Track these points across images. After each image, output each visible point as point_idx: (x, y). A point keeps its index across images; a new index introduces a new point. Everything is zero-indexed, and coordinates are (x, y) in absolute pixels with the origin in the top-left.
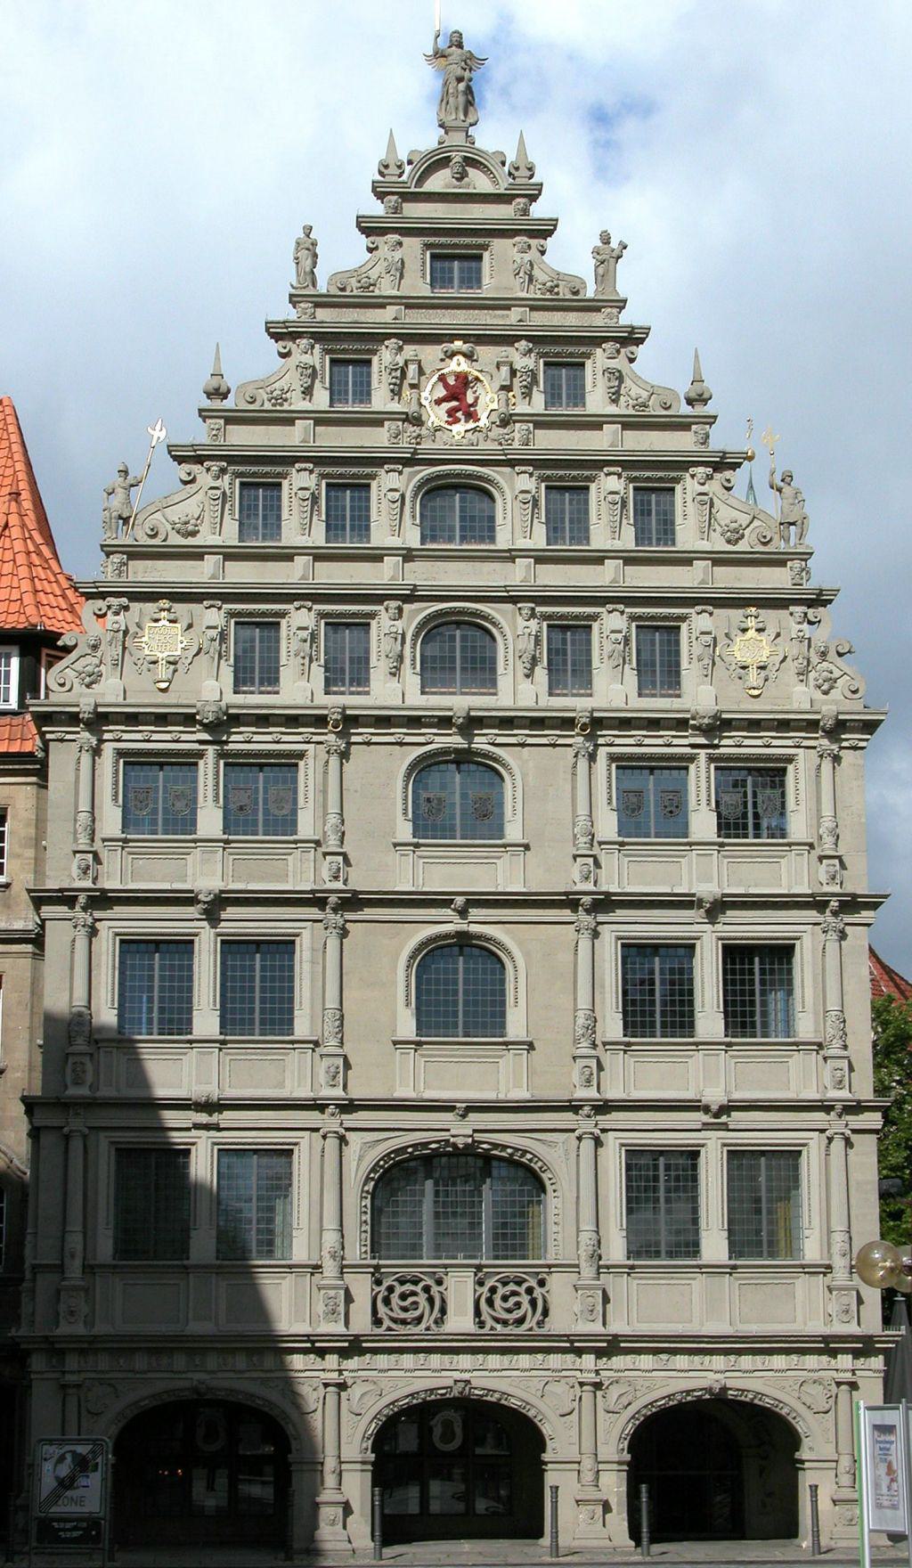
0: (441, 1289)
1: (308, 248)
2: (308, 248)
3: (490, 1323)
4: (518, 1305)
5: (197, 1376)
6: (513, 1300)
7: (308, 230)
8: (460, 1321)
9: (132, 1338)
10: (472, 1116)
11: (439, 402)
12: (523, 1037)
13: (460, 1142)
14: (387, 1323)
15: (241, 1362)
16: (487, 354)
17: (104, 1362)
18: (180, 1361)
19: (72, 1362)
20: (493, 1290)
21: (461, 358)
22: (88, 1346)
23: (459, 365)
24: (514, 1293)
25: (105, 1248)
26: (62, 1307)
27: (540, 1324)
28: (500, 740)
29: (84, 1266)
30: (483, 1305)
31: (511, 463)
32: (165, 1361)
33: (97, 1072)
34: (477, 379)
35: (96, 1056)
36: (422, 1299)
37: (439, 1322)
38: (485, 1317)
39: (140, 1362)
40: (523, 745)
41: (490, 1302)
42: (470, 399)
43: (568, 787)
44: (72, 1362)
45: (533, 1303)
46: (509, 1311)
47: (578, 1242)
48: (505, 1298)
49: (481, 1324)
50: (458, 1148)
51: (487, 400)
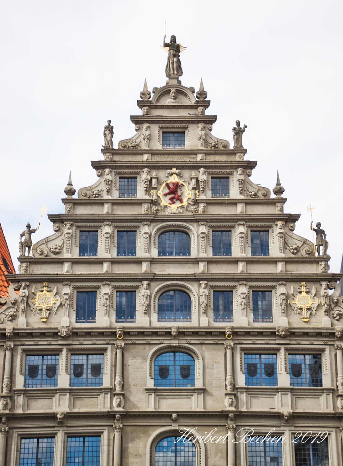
1: (109, 129)
2: (109, 129)
7: (110, 122)
11: (165, 195)
16: (186, 173)
23: (174, 179)
31: (197, 221)
42: (179, 193)
51: (188, 193)
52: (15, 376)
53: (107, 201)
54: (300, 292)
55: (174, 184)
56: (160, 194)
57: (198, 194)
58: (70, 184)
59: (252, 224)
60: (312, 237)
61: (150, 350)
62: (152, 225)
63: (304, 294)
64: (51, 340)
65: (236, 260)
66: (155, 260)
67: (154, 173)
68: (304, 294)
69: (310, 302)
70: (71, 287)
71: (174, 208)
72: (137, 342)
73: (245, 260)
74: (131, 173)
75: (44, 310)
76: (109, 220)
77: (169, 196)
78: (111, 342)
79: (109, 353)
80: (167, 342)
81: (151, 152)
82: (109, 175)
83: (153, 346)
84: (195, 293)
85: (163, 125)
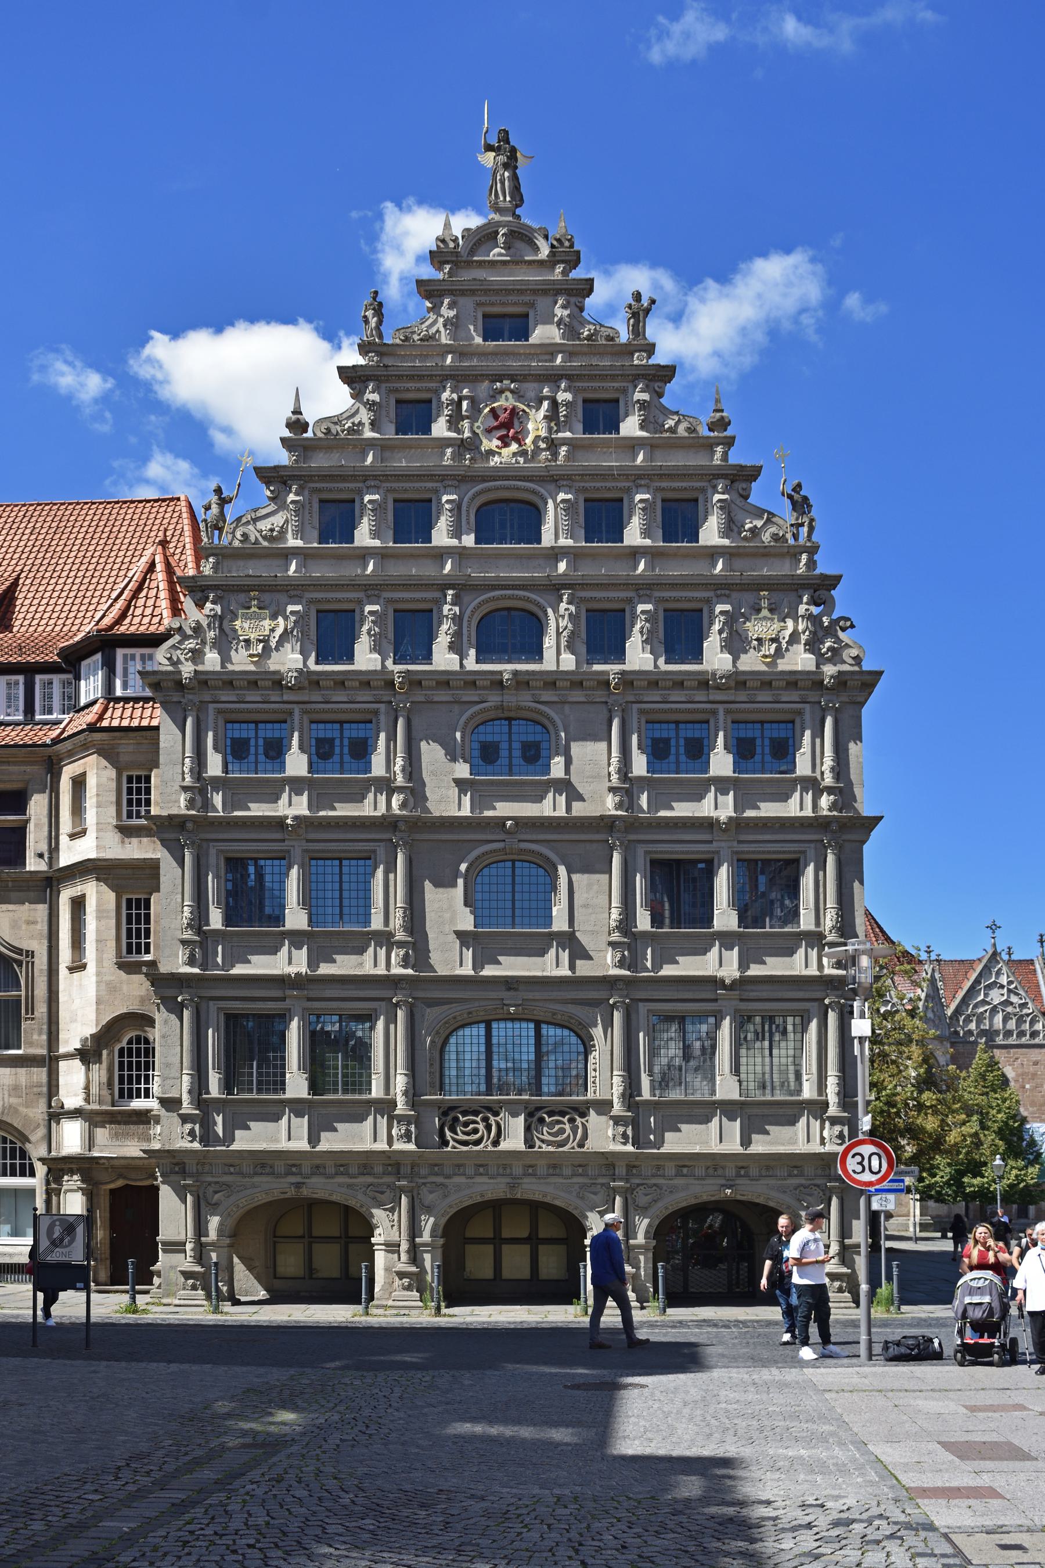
14: (451, 1143)
21: (508, 394)
36: (481, 1127)
54: (759, 611)
59: (664, 484)
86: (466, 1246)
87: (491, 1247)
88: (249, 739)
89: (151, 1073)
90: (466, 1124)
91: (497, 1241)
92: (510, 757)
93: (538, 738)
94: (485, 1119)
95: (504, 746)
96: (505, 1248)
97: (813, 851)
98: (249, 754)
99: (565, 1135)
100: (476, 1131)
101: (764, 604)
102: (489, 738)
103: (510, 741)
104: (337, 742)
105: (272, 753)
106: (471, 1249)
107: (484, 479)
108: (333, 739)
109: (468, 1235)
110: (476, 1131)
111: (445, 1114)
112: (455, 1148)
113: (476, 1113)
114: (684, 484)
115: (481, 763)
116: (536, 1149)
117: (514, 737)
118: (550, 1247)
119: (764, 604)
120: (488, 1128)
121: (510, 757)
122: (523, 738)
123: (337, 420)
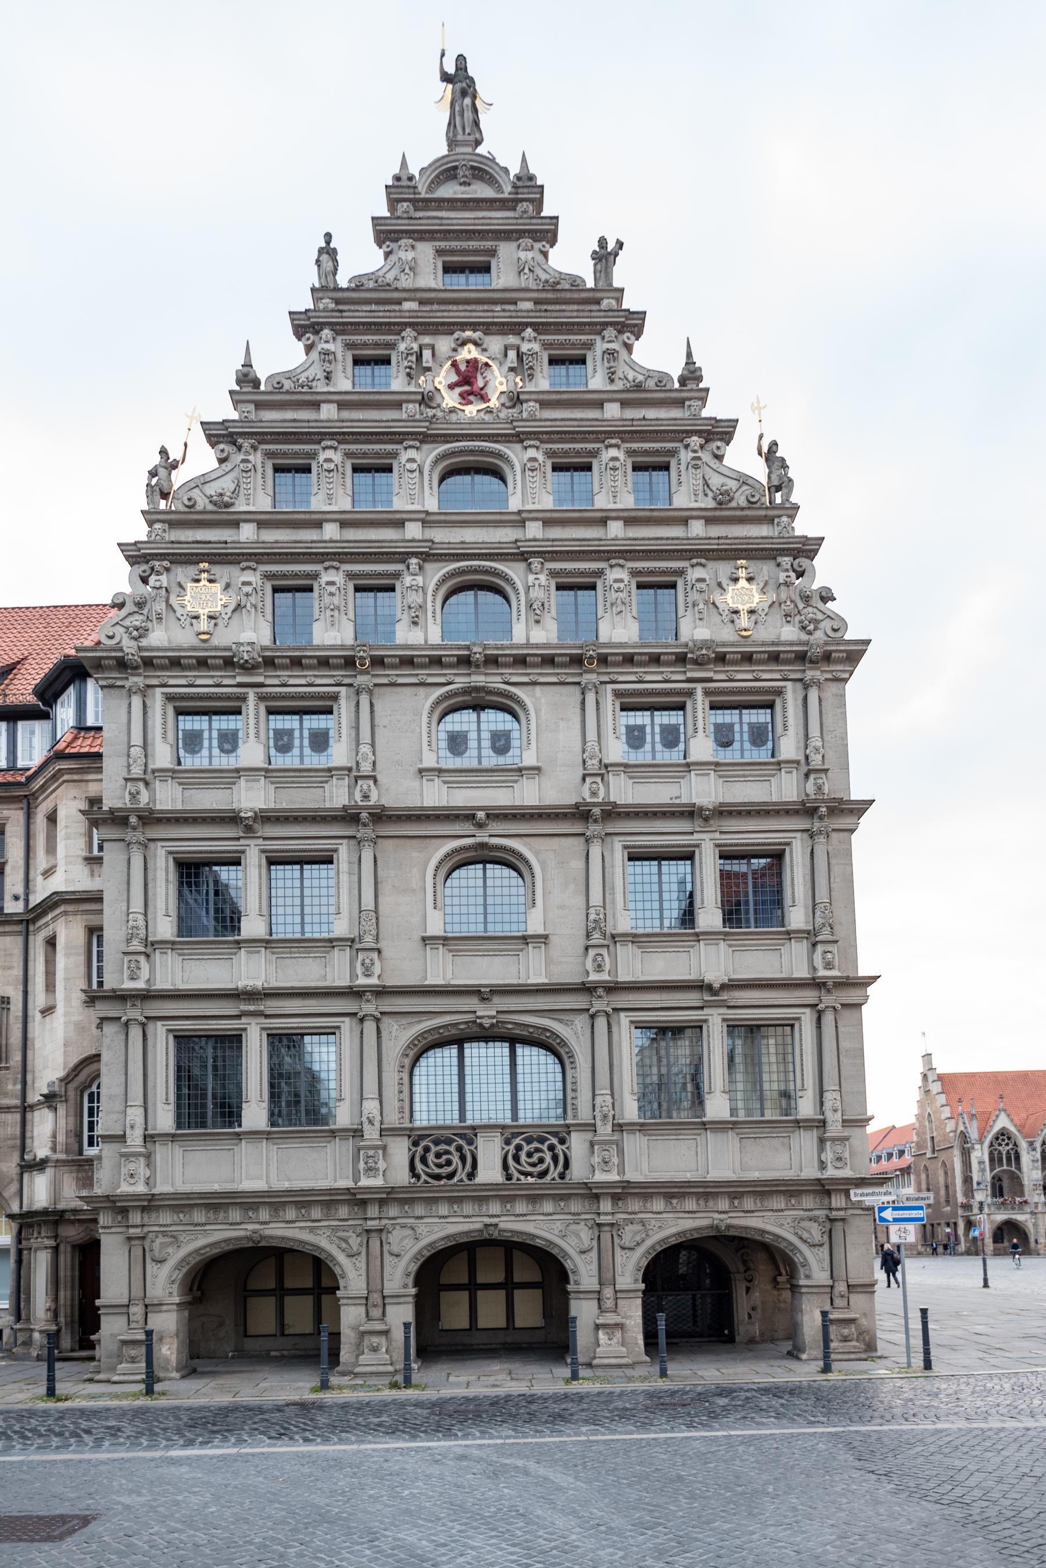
0: (472, 1148)
1: (328, 252)
2: (328, 252)
3: (516, 1175)
4: (541, 1161)
5: (250, 1227)
6: (536, 1156)
7: (328, 237)
8: (490, 1172)
9: (188, 1196)
10: (496, 999)
11: (451, 387)
12: (541, 931)
13: (487, 1022)
14: (424, 1177)
15: (291, 1214)
16: (495, 343)
17: (165, 1218)
18: (235, 1215)
19: (135, 1218)
20: (519, 1148)
21: (471, 346)
22: (150, 1204)
23: (469, 352)
24: (537, 1150)
25: (165, 1119)
26: (124, 1171)
27: (562, 1176)
28: (514, 679)
29: (145, 1137)
30: (511, 1161)
31: (518, 438)
32: (221, 1215)
33: (152, 970)
34: (487, 365)
35: (152, 956)
36: (456, 1159)
37: (471, 1175)
38: (512, 1170)
39: (199, 1216)
40: (534, 683)
41: (517, 1159)
42: (480, 383)
43: (577, 719)
44: (135, 1218)
45: (555, 1158)
46: (534, 1165)
47: (594, 1106)
48: (529, 1155)
49: (509, 1177)
50: (484, 1028)
52: (153, 745)
53: (328, 398)
54: (736, 580)
55: (468, 362)
56: (440, 383)
57: (521, 384)
58: (248, 365)
59: (635, 446)
60: (759, 471)
61: (427, 697)
62: (426, 447)
63: (742, 583)
64: (221, 676)
65: (604, 514)
66: (432, 518)
67: (426, 340)
68: (742, 583)
69: (757, 597)
70: (258, 573)
71: (471, 410)
72: (400, 680)
73: (622, 514)
74: (376, 345)
75: (204, 618)
76: (332, 435)
77: (458, 390)
78: (346, 681)
79: (343, 702)
80: (461, 680)
81: (419, 295)
82: (330, 343)
83: (433, 689)
84: (519, 585)
85: (443, 244)
86: (442, 1293)
87: (467, 1293)
88: (201, 731)
89: (95, 1105)
90: (438, 1155)
91: (473, 1287)
92: (479, 748)
93: (508, 727)
94: (459, 1149)
95: (472, 735)
96: (480, 1294)
97: (799, 842)
98: (201, 748)
99: (544, 1166)
100: (449, 1163)
101: (742, 573)
102: (457, 728)
103: (479, 730)
104: (297, 734)
105: (227, 746)
106: (446, 1297)
107: (447, 438)
108: (292, 730)
109: (444, 1281)
110: (449, 1163)
111: (415, 1144)
112: (427, 1182)
113: (449, 1142)
114: (657, 445)
115: (449, 754)
116: (514, 1181)
117: (483, 726)
118: (530, 1291)
119: (742, 573)
120: (463, 1158)
121: (479, 748)
122: (493, 727)
123: (289, 375)
